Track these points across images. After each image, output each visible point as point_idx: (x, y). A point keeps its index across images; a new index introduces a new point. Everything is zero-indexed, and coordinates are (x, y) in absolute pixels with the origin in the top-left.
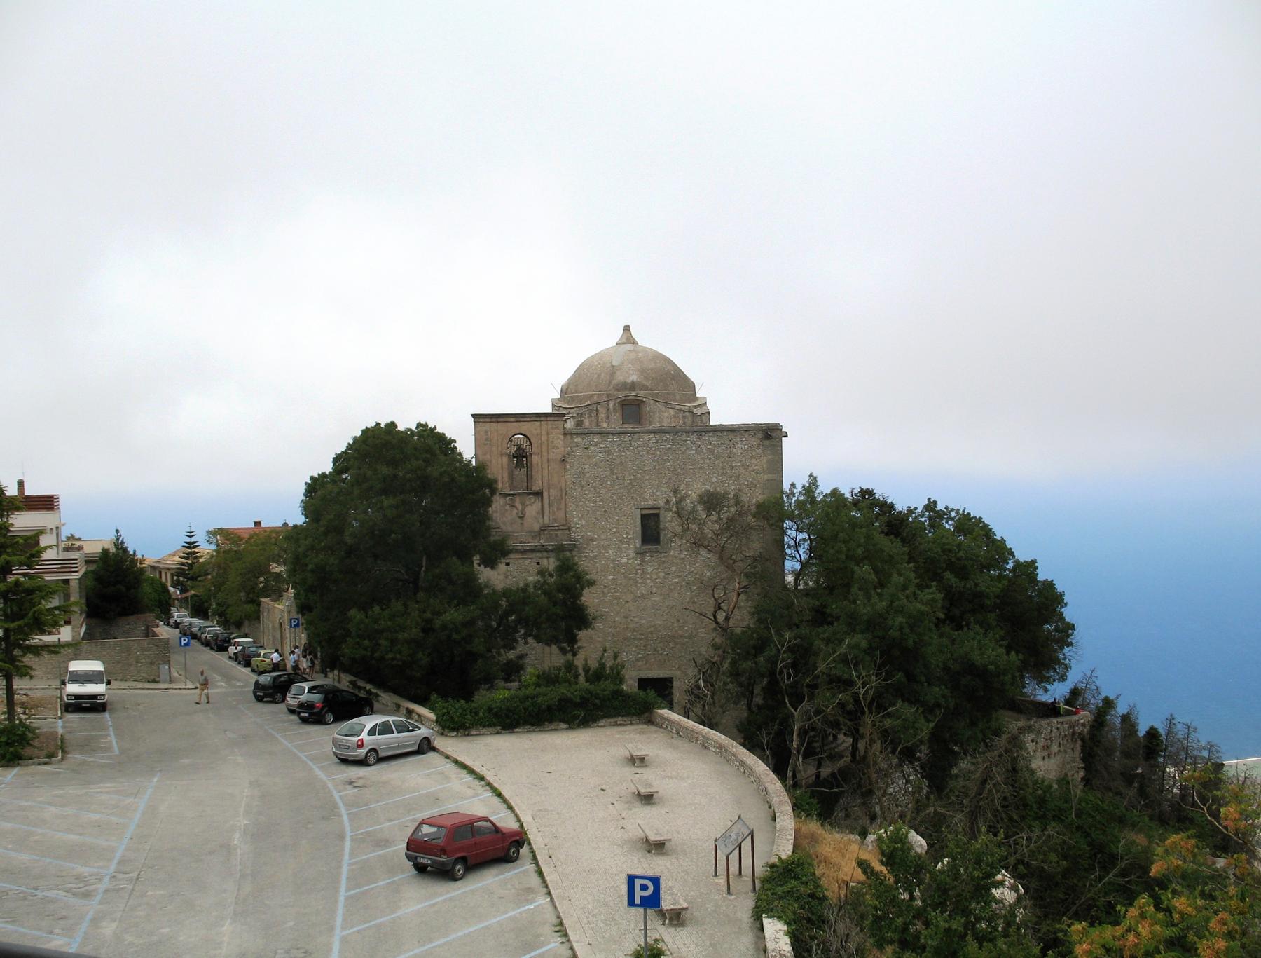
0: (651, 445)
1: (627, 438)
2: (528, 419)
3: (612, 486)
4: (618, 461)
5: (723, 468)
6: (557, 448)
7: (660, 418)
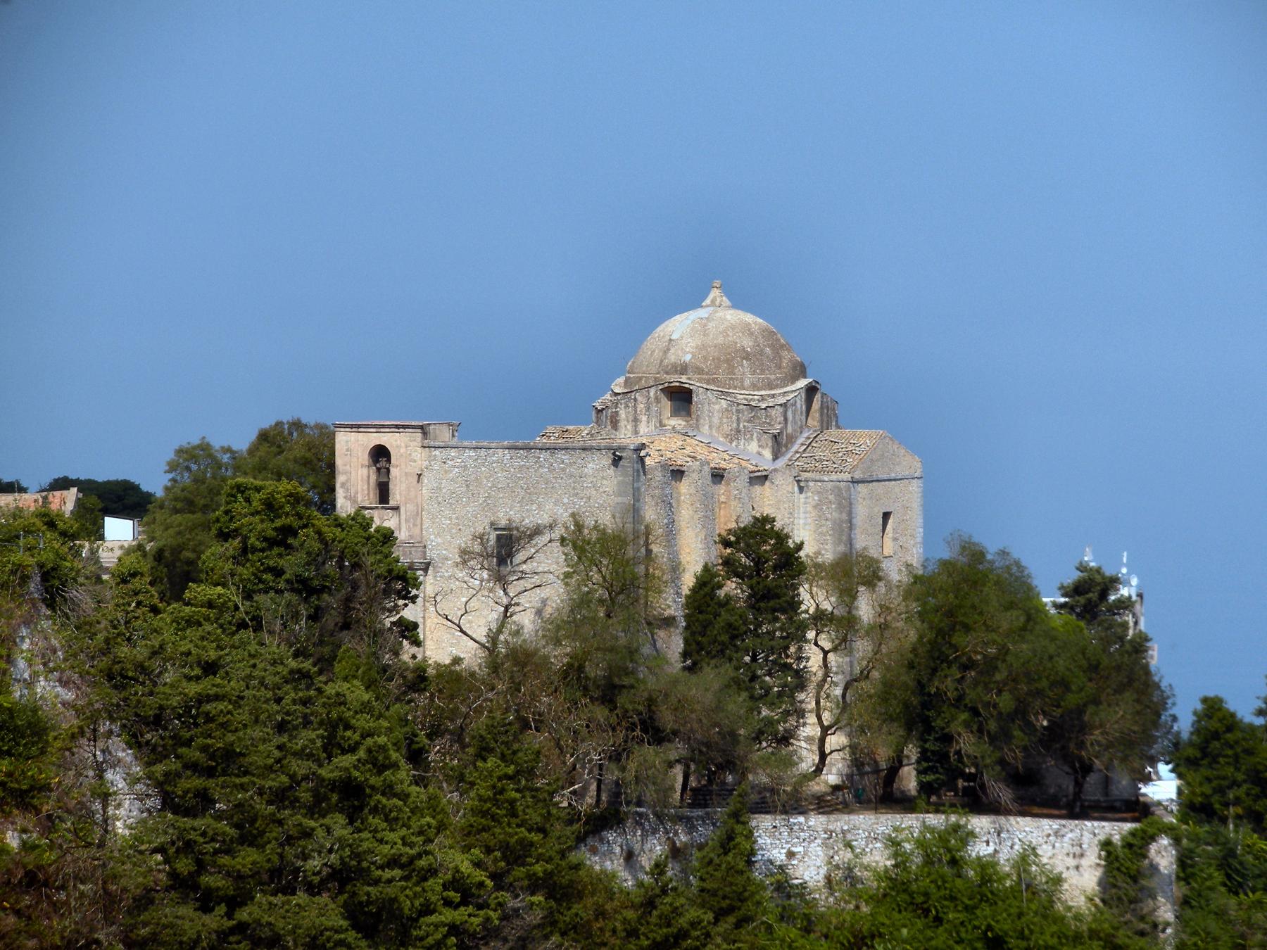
0: (505, 461)
1: (483, 452)
2: (387, 430)
3: (468, 504)
4: (473, 477)
5: (574, 488)
6: (415, 461)
7: (710, 411)
